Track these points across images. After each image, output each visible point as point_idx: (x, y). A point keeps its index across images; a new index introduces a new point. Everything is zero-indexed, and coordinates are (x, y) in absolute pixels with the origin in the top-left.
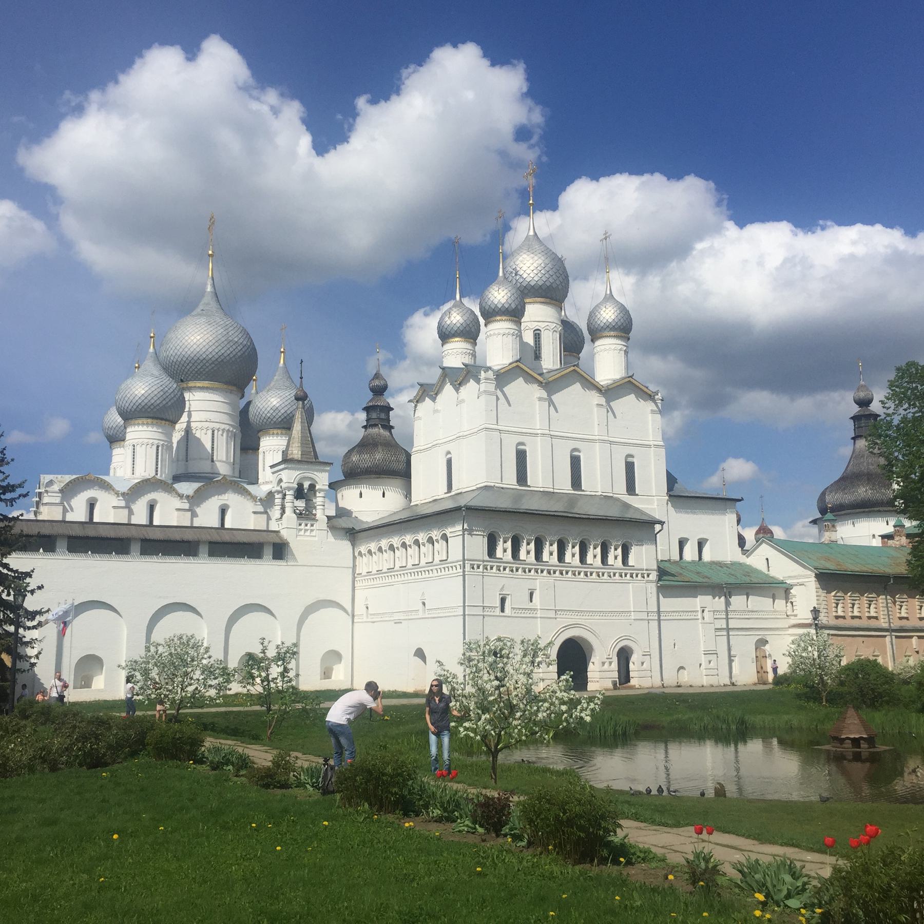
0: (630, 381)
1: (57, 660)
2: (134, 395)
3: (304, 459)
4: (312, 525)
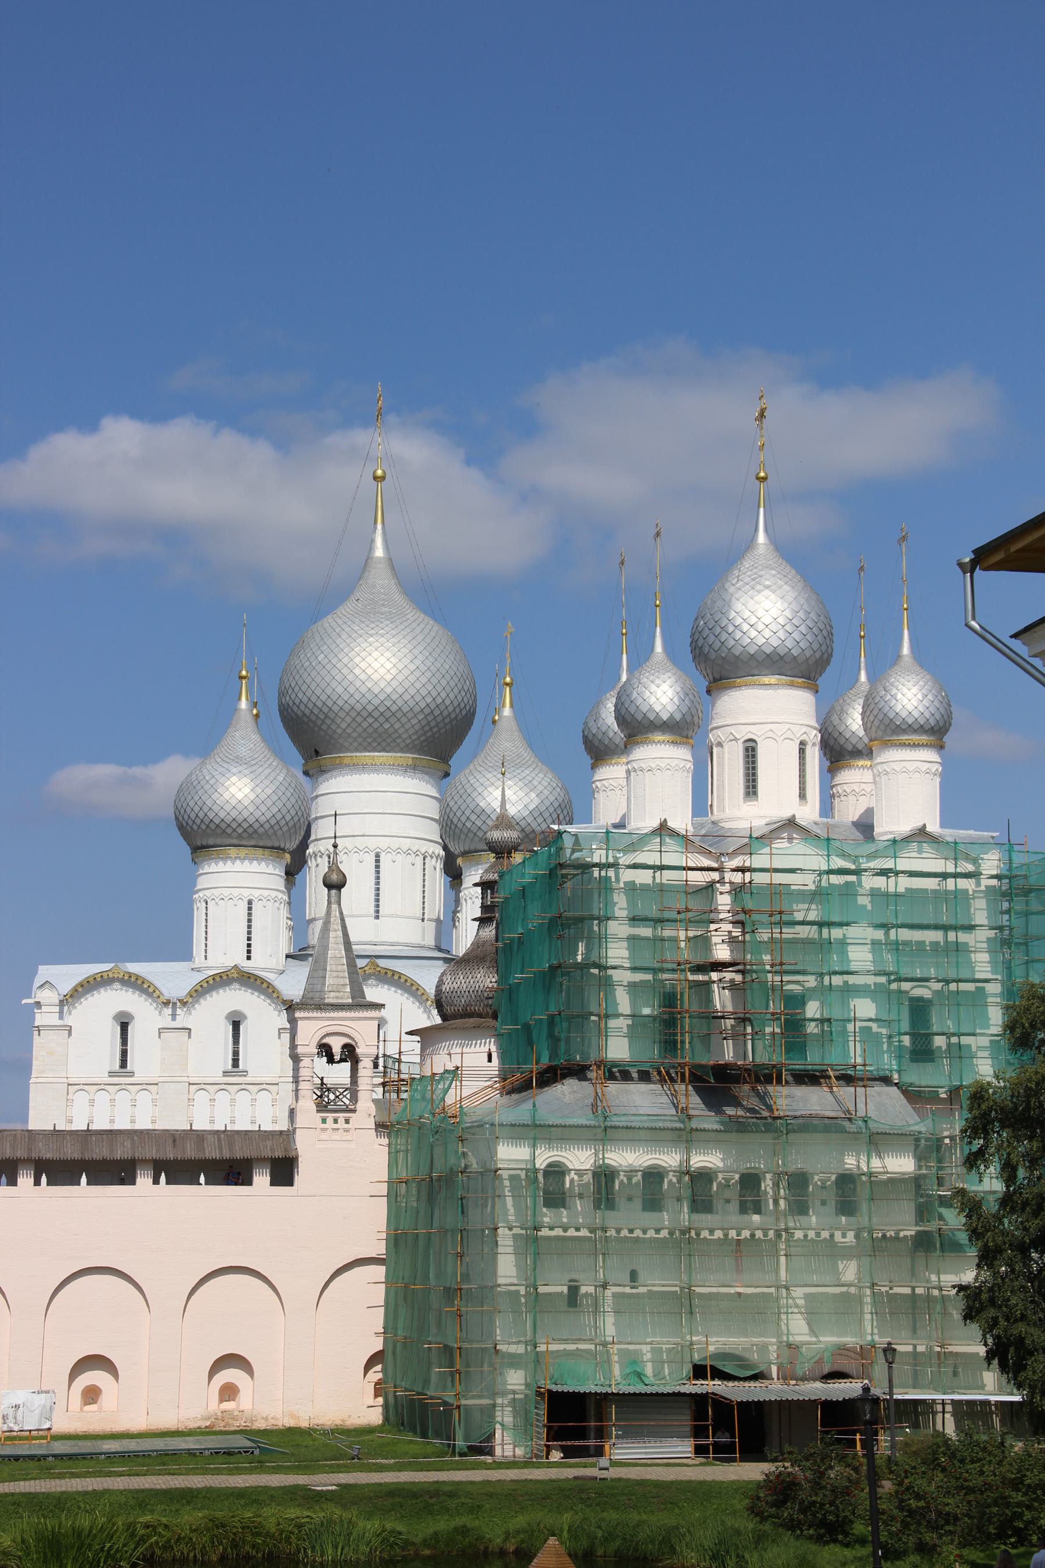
4: (347, 1121)
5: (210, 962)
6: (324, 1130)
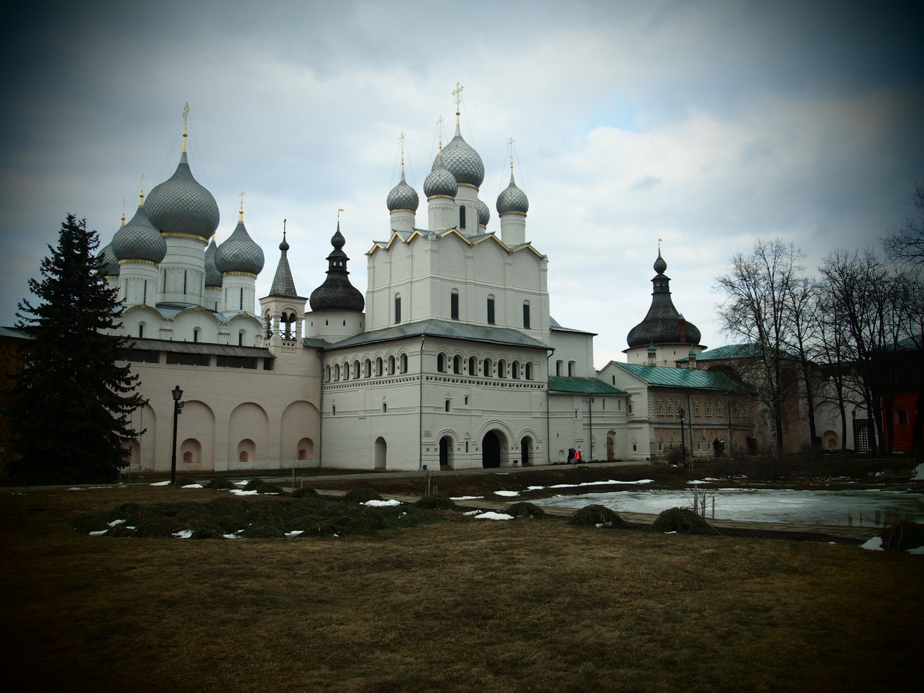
1: (843, 428)
2: (128, 241)
3: (286, 295)
4: (293, 345)
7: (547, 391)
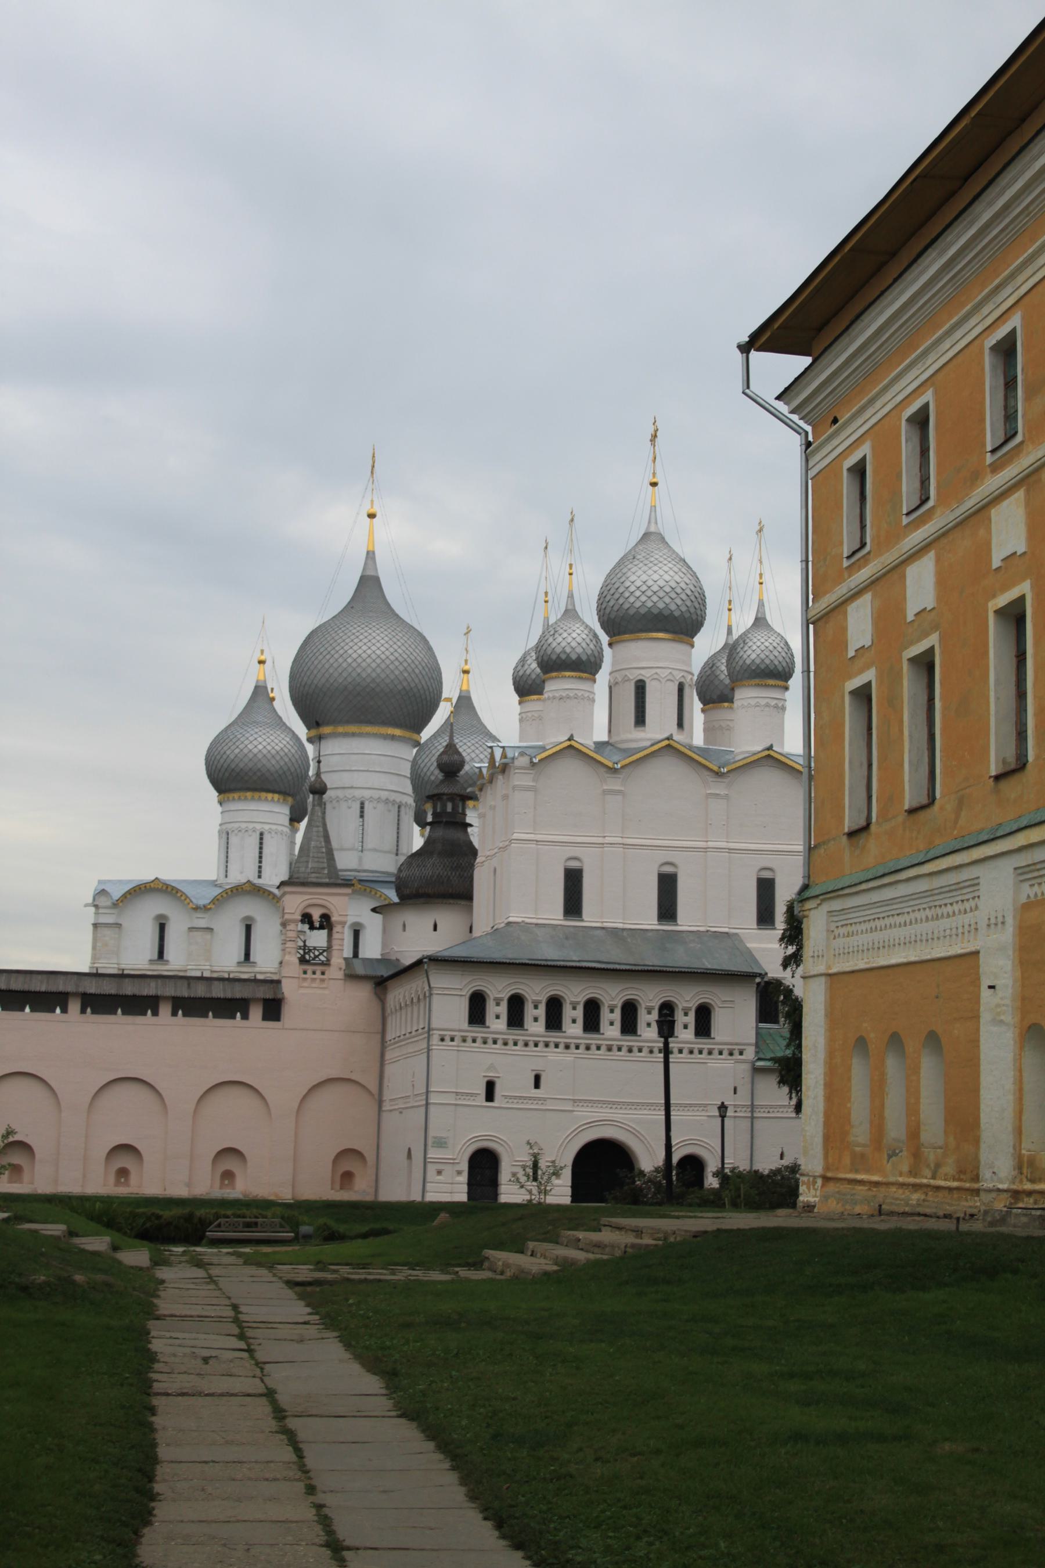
0: (769, 756)
2: (225, 757)
4: (323, 973)
5: (229, 880)
6: (305, 979)
7: (753, 1063)
